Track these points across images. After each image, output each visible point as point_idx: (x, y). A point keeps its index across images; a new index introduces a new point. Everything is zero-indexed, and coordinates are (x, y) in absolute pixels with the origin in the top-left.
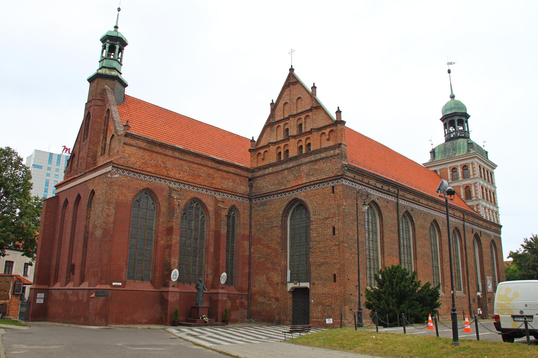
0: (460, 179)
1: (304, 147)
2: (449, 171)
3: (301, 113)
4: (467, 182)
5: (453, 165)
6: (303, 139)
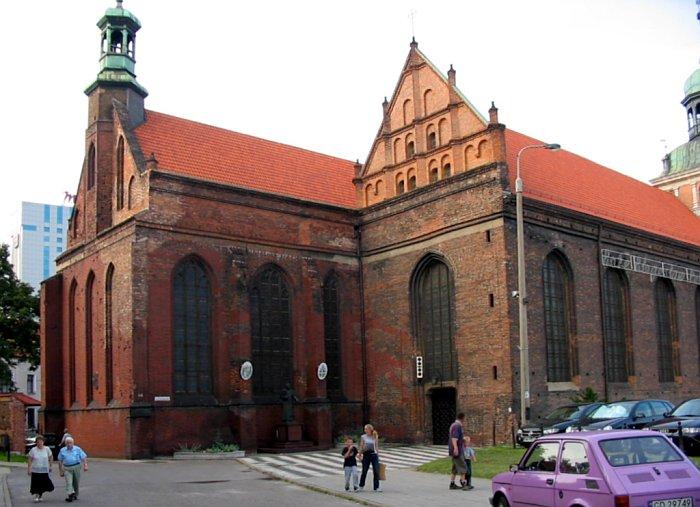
1: (439, 170)
3: (434, 115)
6: (438, 157)
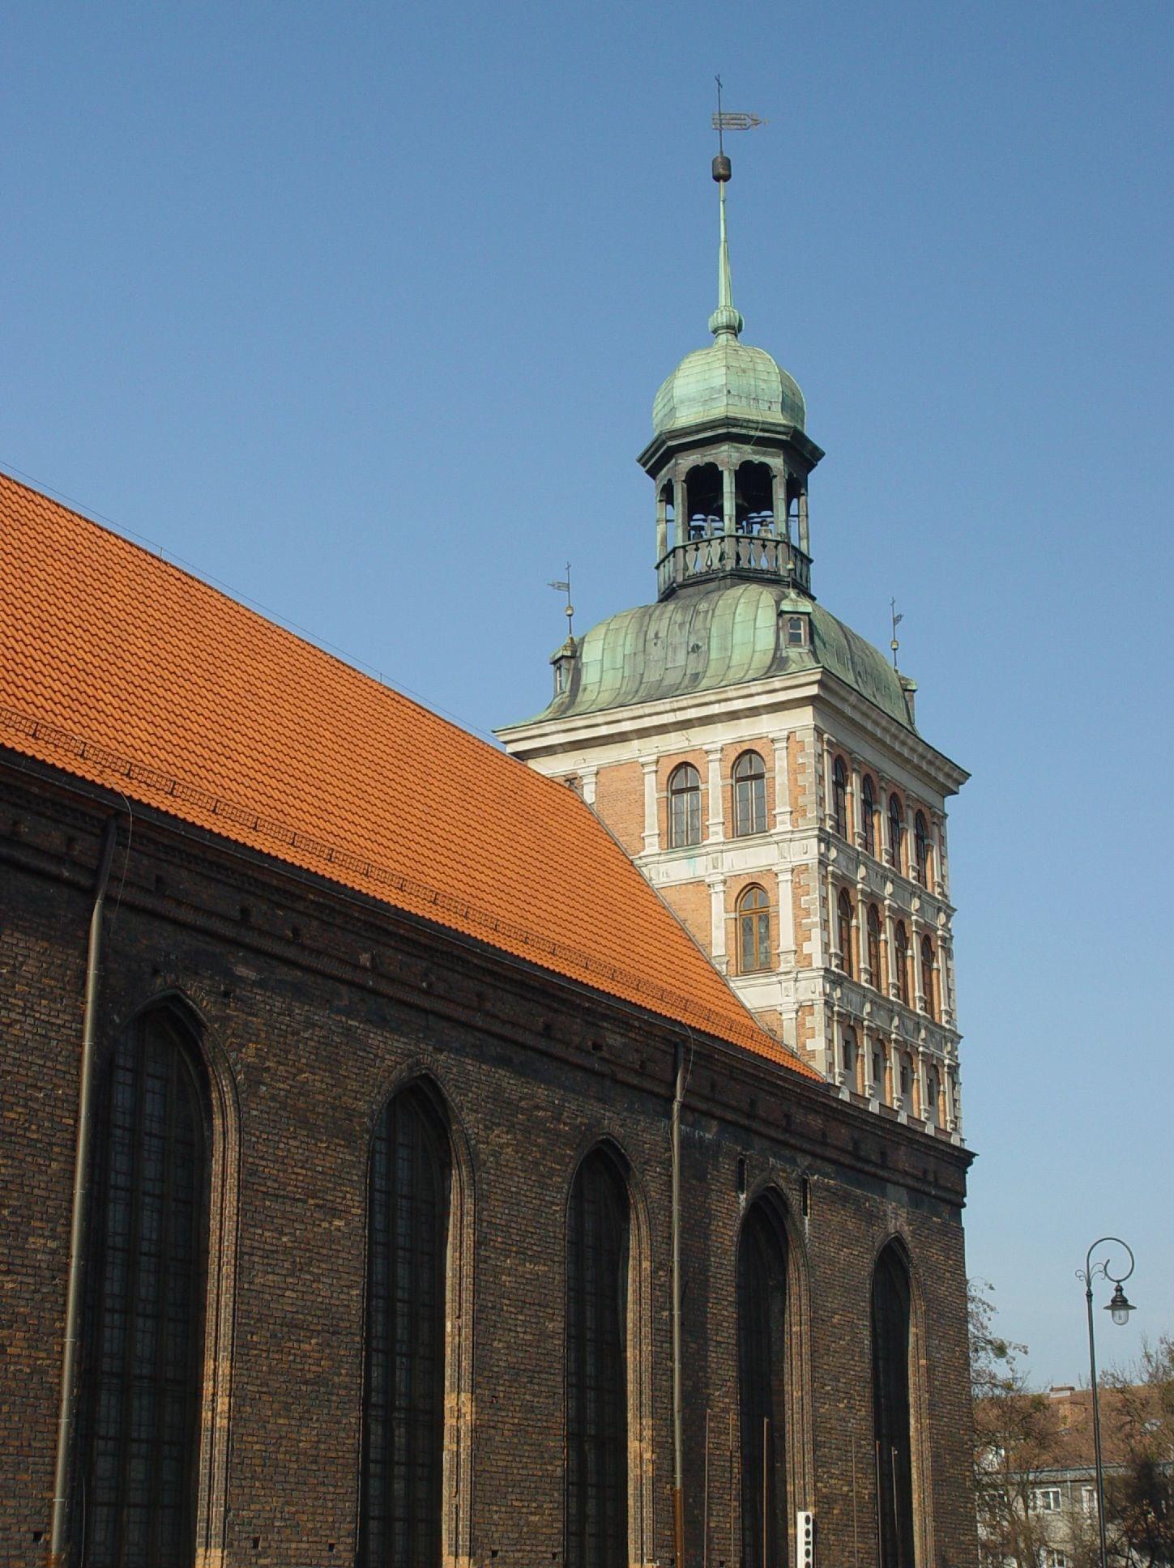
0: (716, 834)
2: (650, 781)
4: (750, 859)
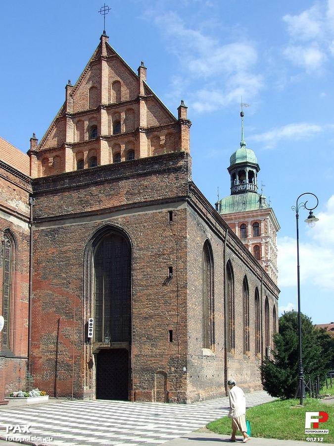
5: (242, 220)
